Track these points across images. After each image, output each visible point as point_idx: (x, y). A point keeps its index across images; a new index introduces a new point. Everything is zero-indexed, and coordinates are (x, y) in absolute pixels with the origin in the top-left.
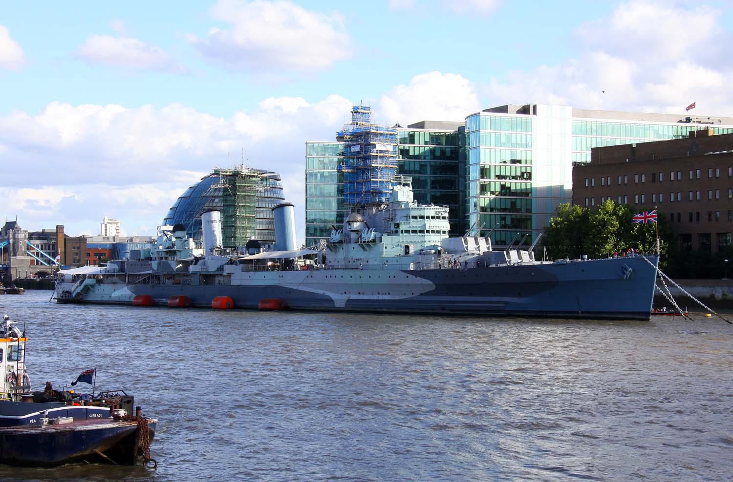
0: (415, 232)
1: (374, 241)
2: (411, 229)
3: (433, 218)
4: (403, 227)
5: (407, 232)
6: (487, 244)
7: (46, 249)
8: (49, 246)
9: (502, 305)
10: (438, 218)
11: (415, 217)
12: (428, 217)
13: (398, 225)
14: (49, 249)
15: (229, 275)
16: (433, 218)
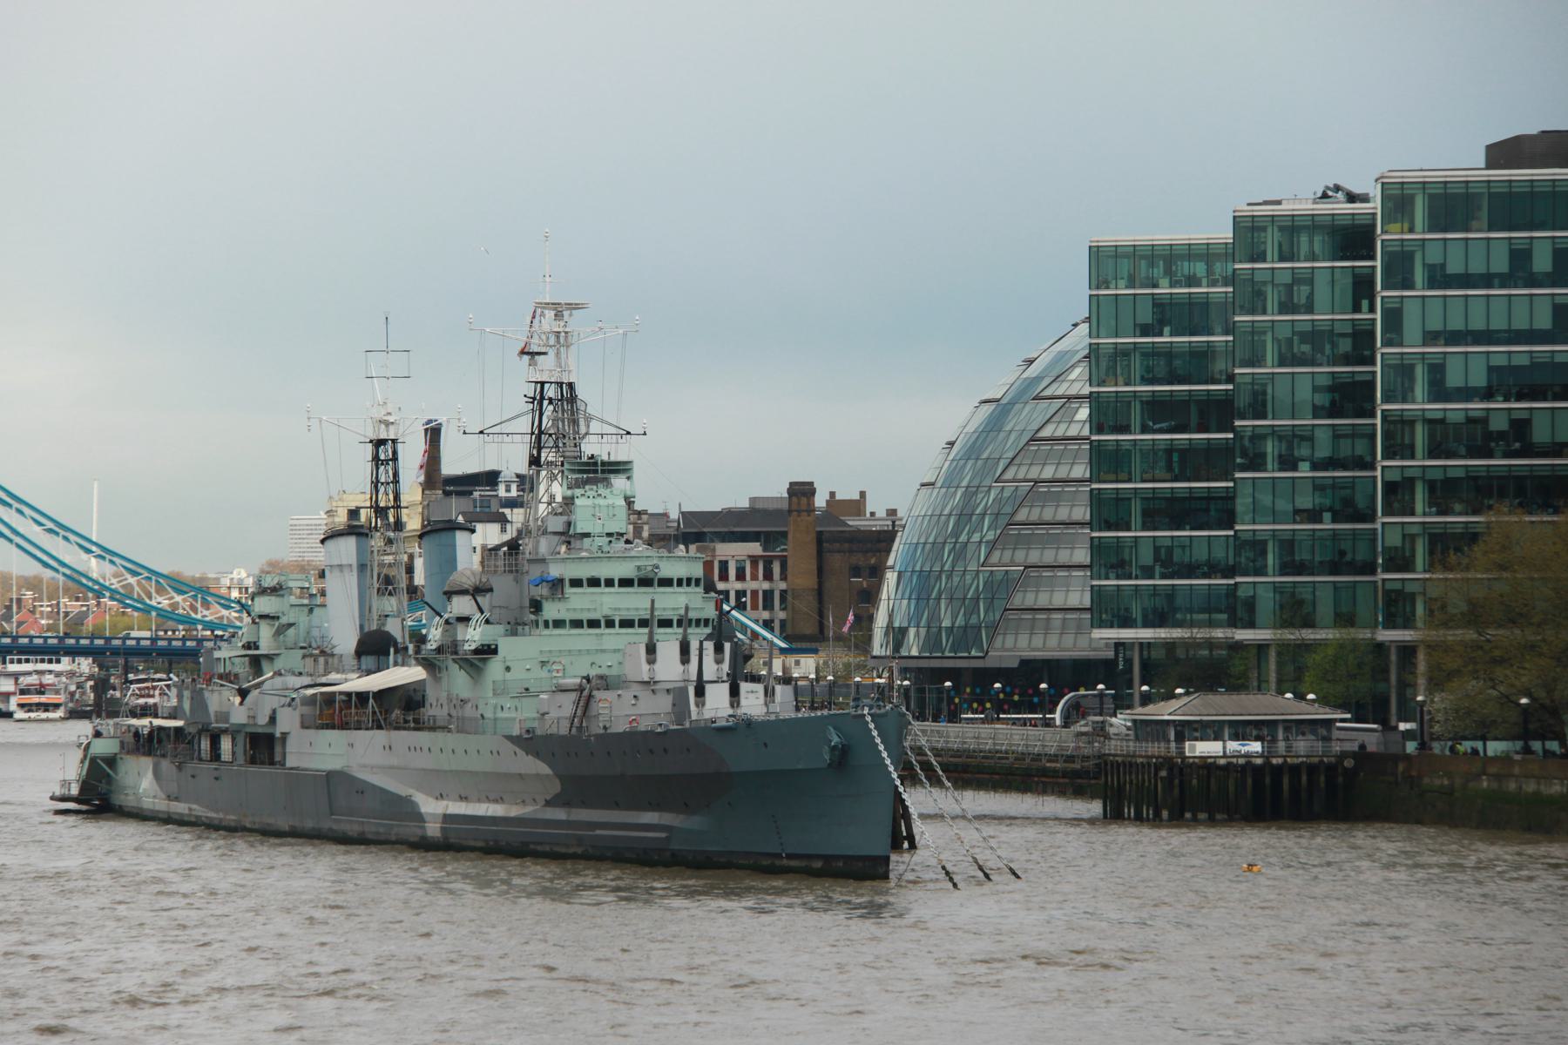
0: (577, 624)
1: (488, 651)
2: (568, 616)
3: (626, 583)
4: (551, 611)
5: (558, 624)
6: (719, 661)
7: (754, 577)
8: (768, 562)
9: (663, 835)
10: (645, 582)
11: (576, 583)
12: (609, 583)
13: (536, 606)
14: (768, 576)
15: (285, 735)
16: (626, 583)
